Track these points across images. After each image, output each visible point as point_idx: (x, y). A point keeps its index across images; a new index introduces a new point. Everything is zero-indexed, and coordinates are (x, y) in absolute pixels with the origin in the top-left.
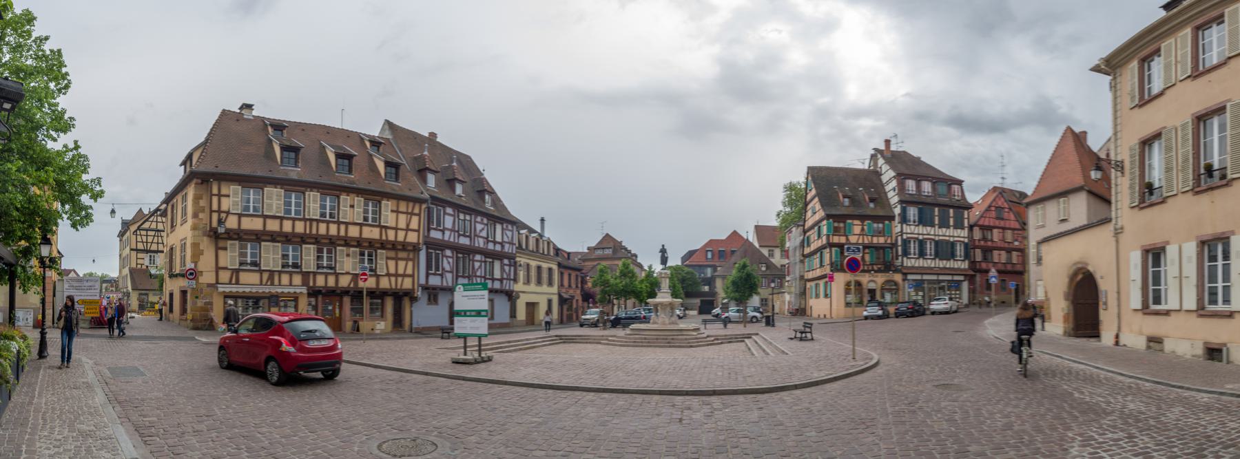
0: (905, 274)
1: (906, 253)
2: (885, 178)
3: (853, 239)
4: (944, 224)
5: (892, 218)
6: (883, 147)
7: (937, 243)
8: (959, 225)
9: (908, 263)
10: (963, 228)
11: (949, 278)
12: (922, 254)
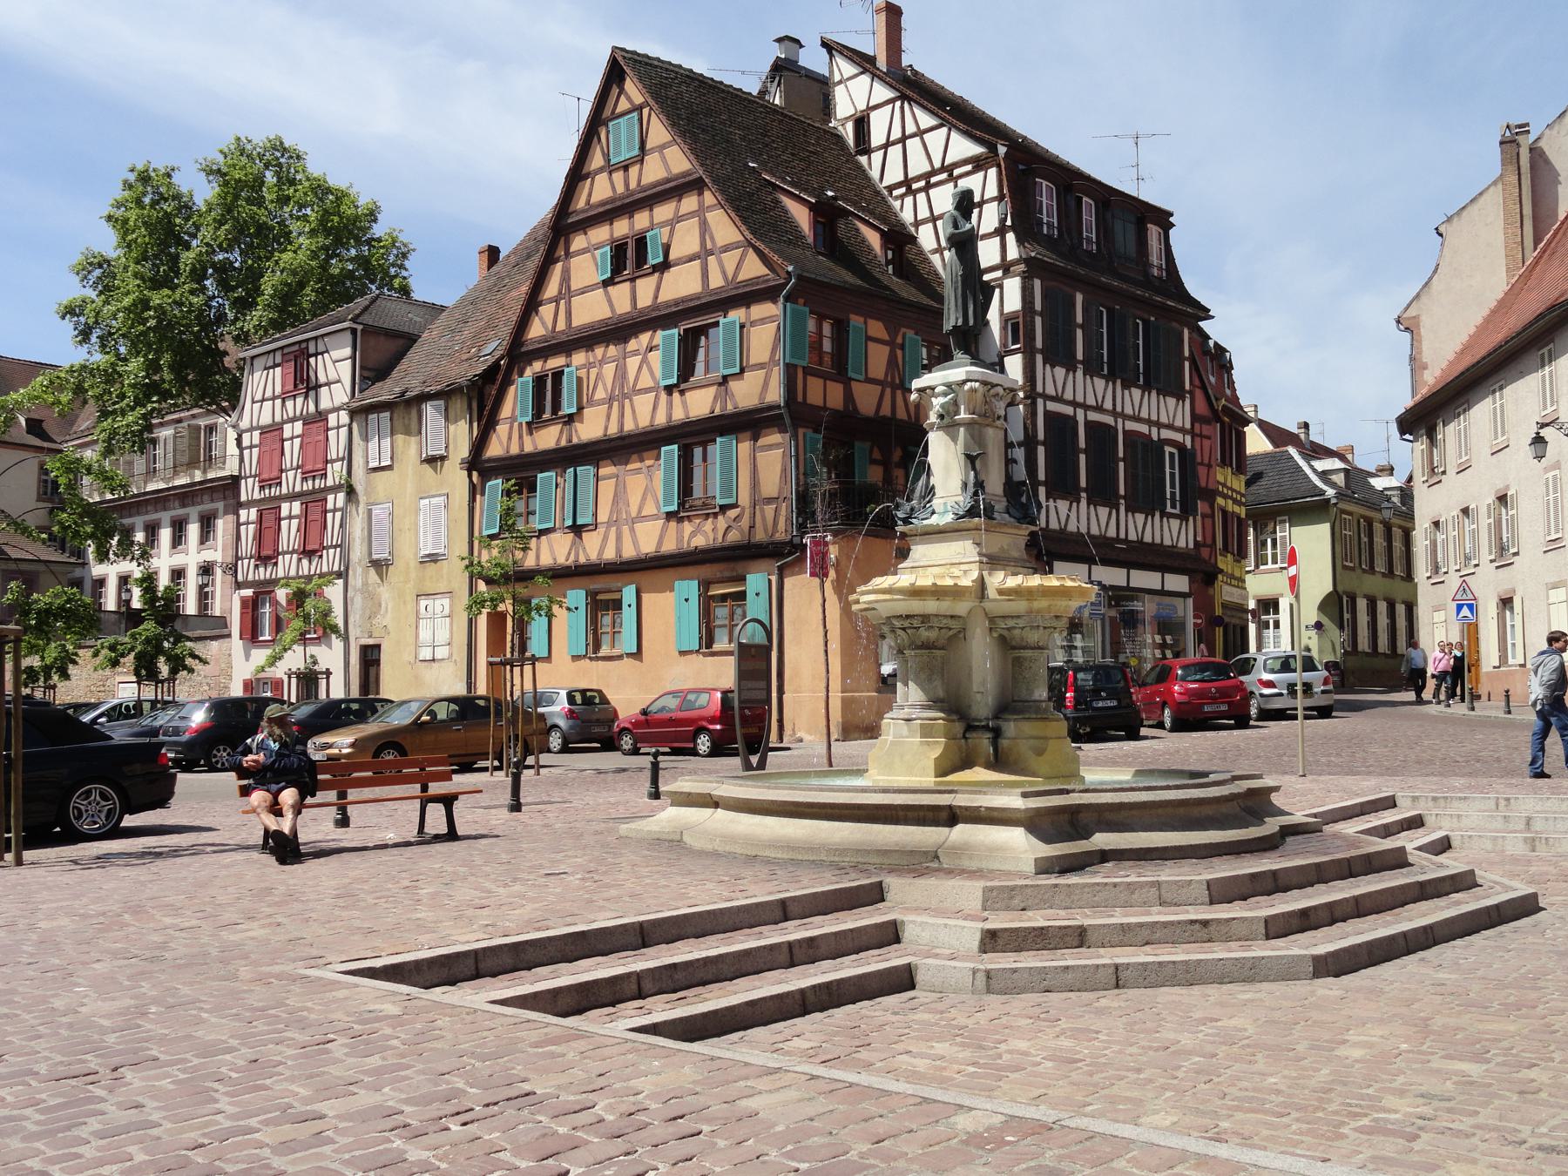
2: (885, 169)
10: (1180, 396)
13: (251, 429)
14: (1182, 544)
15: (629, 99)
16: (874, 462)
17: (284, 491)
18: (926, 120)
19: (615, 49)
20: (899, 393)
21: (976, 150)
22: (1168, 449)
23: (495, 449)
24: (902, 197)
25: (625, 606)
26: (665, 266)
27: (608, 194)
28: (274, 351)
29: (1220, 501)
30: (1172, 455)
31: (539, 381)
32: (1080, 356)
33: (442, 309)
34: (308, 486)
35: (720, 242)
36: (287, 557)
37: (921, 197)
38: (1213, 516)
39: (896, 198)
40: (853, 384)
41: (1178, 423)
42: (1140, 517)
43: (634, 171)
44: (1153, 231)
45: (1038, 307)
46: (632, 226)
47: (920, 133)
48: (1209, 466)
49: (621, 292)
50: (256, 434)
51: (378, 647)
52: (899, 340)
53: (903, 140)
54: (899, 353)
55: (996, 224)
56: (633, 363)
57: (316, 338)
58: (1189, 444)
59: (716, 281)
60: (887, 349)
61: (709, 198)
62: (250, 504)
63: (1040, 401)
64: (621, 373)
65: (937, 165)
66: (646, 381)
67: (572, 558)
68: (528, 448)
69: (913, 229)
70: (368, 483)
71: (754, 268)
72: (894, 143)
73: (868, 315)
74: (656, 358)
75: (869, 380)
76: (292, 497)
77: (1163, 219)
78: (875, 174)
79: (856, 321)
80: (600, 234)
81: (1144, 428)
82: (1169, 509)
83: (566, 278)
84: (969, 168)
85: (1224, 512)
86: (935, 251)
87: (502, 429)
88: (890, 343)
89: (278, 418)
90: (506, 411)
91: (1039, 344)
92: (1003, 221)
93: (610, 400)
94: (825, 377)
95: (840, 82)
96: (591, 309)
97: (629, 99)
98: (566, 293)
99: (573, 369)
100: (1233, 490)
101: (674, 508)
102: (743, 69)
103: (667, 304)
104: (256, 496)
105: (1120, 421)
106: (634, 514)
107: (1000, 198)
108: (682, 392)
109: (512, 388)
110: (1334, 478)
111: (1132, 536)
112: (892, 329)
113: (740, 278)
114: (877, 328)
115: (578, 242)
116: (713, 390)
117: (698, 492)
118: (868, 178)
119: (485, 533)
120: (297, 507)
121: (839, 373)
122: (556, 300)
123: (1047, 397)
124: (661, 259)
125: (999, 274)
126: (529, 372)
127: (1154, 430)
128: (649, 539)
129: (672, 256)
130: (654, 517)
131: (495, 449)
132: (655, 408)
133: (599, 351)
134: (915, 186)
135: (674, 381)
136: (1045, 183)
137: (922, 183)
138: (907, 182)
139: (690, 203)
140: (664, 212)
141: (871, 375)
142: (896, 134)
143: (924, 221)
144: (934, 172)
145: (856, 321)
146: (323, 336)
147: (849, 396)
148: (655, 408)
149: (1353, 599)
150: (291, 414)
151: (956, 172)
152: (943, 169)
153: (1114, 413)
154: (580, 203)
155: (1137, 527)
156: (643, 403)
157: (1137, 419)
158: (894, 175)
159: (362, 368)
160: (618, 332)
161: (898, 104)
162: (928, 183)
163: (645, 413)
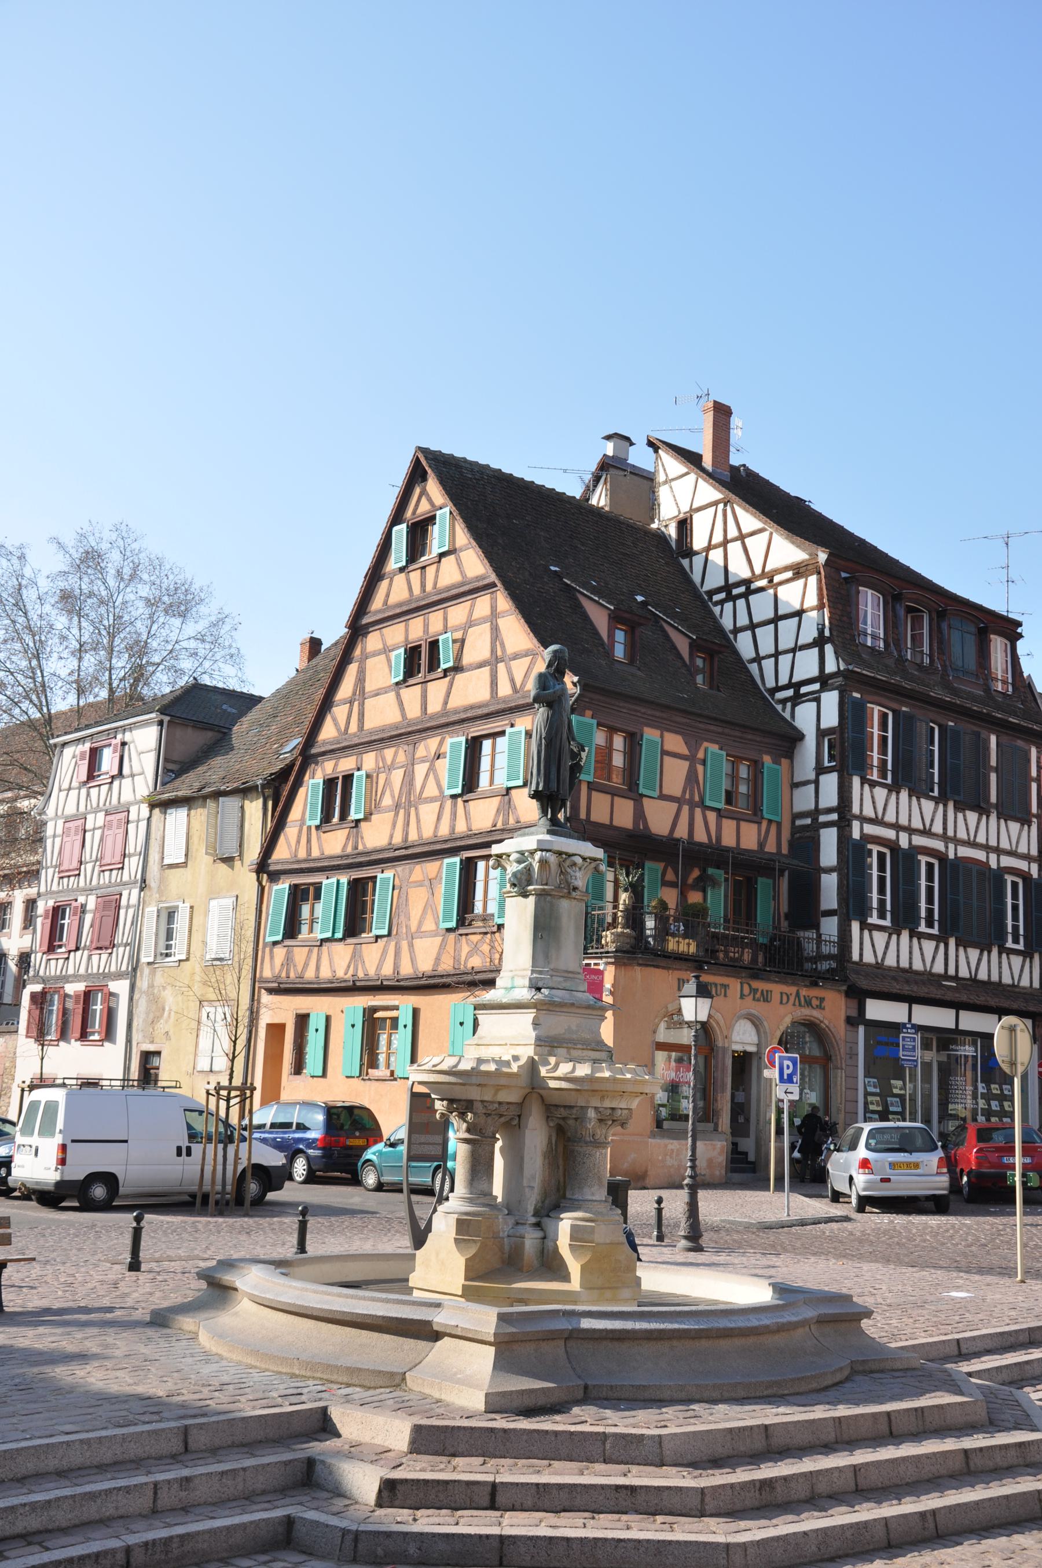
0: (858, 995)
1: (854, 905)
3: (660, 819)
7: (953, 871)
8: (1013, 809)
9: (874, 946)
10: (1025, 820)
12: (904, 918)
14: (1025, 982)
20: (698, 811)
22: (1009, 879)
23: (282, 853)
24: (722, 602)
26: (457, 669)
30: (1015, 885)
31: (330, 783)
33: (259, 699)
35: (510, 650)
37: (741, 603)
39: (716, 604)
40: (645, 801)
41: (1023, 849)
42: (974, 954)
44: (998, 644)
46: (426, 626)
49: (411, 695)
51: (158, 1053)
52: (701, 755)
54: (700, 768)
55: (815, 634)
56: (421, 770)
59: (504, 690)
60: (686, 764)
61: (503, 602)
63: (856, 825)
64: (409, 778)
65: (758, 571)
66: (431, 790)
67: (351, 972)
68: (315, 853)
69: (731, 636)
70: (162, 880)
72: (716, 547)
73: (664, 727)
74: (443, 765)
75: (663, 797)
76: (88, 890)
77: (1010, 629)
78: (696, 577)
79: (650, 734)
80: (396, 635)
81: (980, 855)
82: (1010, 944)
83: (361, 679)
84: (789, 574)
86: (753, 661)
87: (290, 831)
88: (691, 758)
90: (295, 814)
92: (821, 632)
93: (397, 807)
94: (614, 793)
95: (666, 482)
96: (382, 713)
99: (363, 773)
101: (453, 924)
102: (562, 469)
103: (456, 712)
104: (55, 888)
105: (951, 846)
109: (302, 791)
111: (964, 973)
112: (693, 743)
114: (675, 742)
116: (496, 801)
117: (478, 908)
118: (689, 581)
121: (630, 790)
123: (864, 819)
125: (816, 686)
127: (993, 857)
128: (425, 956)
130: (434, 934)
132: (439, 819)
133: (389, 753)
134: (735, 592)
135: (459, 791)
136: (870, 592)
138: (727, 588)
139: (482, 605)
140: (457, 613)
141: (665, 792)
142: (718, 538)
144: (755, 577)
145: (650, 734)
147: (639, 814)
148: (439, 819)
153: (944, 837)
154: (377, 603)
155: (969, 962)
157: (973, 844)
158: (715, 580)
159: (166, 760)
161: (721, 506)
162: (748, 588)
163: (429, 823)
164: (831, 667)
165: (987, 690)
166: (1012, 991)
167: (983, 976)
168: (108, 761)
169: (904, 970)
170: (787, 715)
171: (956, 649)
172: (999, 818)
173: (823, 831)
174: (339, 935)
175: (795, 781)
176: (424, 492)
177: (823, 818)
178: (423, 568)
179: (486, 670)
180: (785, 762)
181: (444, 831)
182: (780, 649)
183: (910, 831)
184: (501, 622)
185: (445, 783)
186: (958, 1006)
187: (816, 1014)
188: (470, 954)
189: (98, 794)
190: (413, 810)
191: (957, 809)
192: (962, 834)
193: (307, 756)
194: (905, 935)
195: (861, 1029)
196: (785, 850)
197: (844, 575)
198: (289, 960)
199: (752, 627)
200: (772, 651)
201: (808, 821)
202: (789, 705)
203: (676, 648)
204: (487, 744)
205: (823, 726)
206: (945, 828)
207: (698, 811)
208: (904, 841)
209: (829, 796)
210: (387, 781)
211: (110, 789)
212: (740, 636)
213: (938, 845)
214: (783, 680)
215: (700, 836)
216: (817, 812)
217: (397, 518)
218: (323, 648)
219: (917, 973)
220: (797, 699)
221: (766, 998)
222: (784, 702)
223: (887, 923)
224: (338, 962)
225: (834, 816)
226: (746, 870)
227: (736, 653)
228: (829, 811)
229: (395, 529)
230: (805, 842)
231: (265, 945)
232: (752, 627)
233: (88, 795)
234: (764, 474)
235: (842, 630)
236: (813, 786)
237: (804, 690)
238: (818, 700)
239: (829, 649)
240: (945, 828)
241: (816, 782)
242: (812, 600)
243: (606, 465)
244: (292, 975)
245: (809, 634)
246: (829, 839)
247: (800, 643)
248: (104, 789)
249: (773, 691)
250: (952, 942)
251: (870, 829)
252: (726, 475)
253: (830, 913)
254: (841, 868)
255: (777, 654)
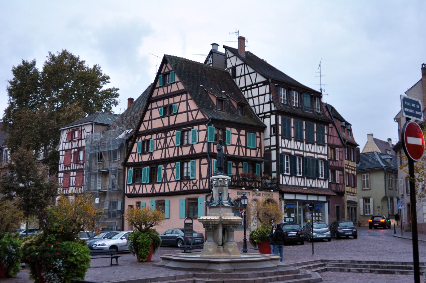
1: (280, 170)
2: (241, 83)
3: (231, 150)
4: (310, 141)
5: (263, 128)
6: (235, 45)
7: (305, 160)
8: (321, 143)
10: (324, 146)
11: (314, 198)
12: (293, 173)
13: (62, 150)
15: (168, 68)
16: (233, 167)
17: (72, 169)
18: (251, 70)
19: (164, 55)
20: (240, 148)
21: (264, 79)
23: (130, 160)
24: (244, 91)
25: (166, 205)
26: (177, 113)
27: (162, 93)
28: (70, 128)
29: (347, 170)
31: (143, 142)
32: (293, 136)
34: (78, 167)
35: (192, 109)
36: (72, 188)
37: (249, 91)
38: (343, 175)
39: (243, 91)
40: (228, 147)
41: (323, 153)
42: (311, 181)
43: (169, 87)
45: (280, 123)
47: (249, 74)
48: (342, 160)
49: (165, 120)
50: (64, 152)
53: (245, 75)
54: (241, 137)
56: (169, 139)
57: (82, 126)
58: (326, 159)
59: (191, 119)
60: (237, 136)
61: (189, 97)
62: (61, 172)
63: (280, 149)
64: (165, 142)
65: (254, 83)
66: (172, 144)
67: (152, 191)
68: (140, 160)
71: (200, 116)
73: (231, 127)
74: (174, 138)
75: (232, 145)
76: (73, 170)
78: (238, 84)
80: (160, 103)
81: (312, 155)
83: (151, 114)
84: (262, 84)
85: (348, 173)
86: (253, 107)
88: (239, 135)
89: (70, 148)
90: (134, 150)
91: (280, 133)
92: (270, 100)
93: (162, 149)
96: (157, 124)
97: (168, 68)
98: (151, 119)
99: (152, 140)
100: (351, 166)
104: (63, 170)
105: (305, 153)
106: (168, 180)
107: (270, 93)
108: (181, 148)
109: (136, 145)
110: (387, 160)
111: (309, 185)
113: (197, 118)
114: (234, 131)
115: (154, 105)
117: (185, 175)
118: (236, 85)
119: (128, 183)
120: (75, 173)
122: (148, 121)
123: (282, 148)
124: (176, 112)
125: (269, 114)
126: (140, 140)
127: (316, 155)
128: (172, 187)
129: (179, 111)
131: (130, 160)
133: (160, 135)
134: (248, 88)
135: (179, 145)
137: (250, 88)
138: (246, 87)
139: (184, 97)
140: (177, 99)
142: (243, 73)
143: (250, 98)
144: (253, 85)
145: (228, 129)
146: (83, 125)
149: (392, 199)
150: (74, 147)
151: (259, 85)
152: (255, 84)
153: (303, 151)
154: (154, 95)
156: (171, 150)
157: (310, 152)
158: (242, 85)
160: (165, 130)
161: (243, 65)
162: (251, 87)
163: (171, 153)
164: (273, 109)
165: (313, 111)
166: (321, 189)
167: (313, 186)
168: (77, 134)
169: (293, 186)
170: (262, 121)
171: (305, 102)
172: (317, 145)
173: (272, 151)
174: (148, 182)
175: (265, 138)
176: (167, 66)
177: (272, 148)
178: (167, 87)
179: (186, 113)
180: (262, 134)
181: (176, 155)
182: (260, 103)
183: (294, 150)
184: (189, 101)
185: (175, 143)
186: (307, 194)
187: (271, 198)
188: (184, 187)
189: (75, 145)
190: (167, 150)
191: (307, 143)
192: (308, 150)
193: (137, 134)
194: (293, 177)
195: (283, 202)
196: (263, 156)
197: (276, 84)
198: (134, 188)
199: (253, 98)
200: (258, 104)
201: (268, 149)
202: (263, 118)
203: (233, 105)
204: (186, 133)
205: (272, 124)
206: (303, 149)
207: (240, 148)
208: (293, 153)
209: (274, 142)
210: (160, 142)
211: (78, 142)
212: (249, 100)
213: (301, 153)
214: (261, 112)
215: (241, 154)
216: (270, 146)
217: (159, 73)
218: (134, 101)
219: (297, 186)
220: (265, 117)
221: (259, 195)
222: (261, 118)
223: (289, 174)
224: (148, 189)
225: (275, 147)
226: (252, 162)
227: (249, 104)
228: (274, 146)
229: (159, 76)
230: (268, 154)
231: (127, 185)
232: (253, 98)
233: (72, 144)
234: (254, 54)
235: (275, 100)
236: (269, 140)
237: (266, 115)
238: (270, 117)
239: (272, 104)
240: (303, 149)
241: (270, 139)
242: (268, 91)
243: (211, 53)
244: (135, 193)
245: (267, 100)
246: (274, 153)
247: (265, 102)
248: (77, 143)
249: (258, 115)
250: (306, 179)
251: (284, 150)
252: (243, 56)
253: (274, 172)
254: (277, 161)
255: (259, 105)
